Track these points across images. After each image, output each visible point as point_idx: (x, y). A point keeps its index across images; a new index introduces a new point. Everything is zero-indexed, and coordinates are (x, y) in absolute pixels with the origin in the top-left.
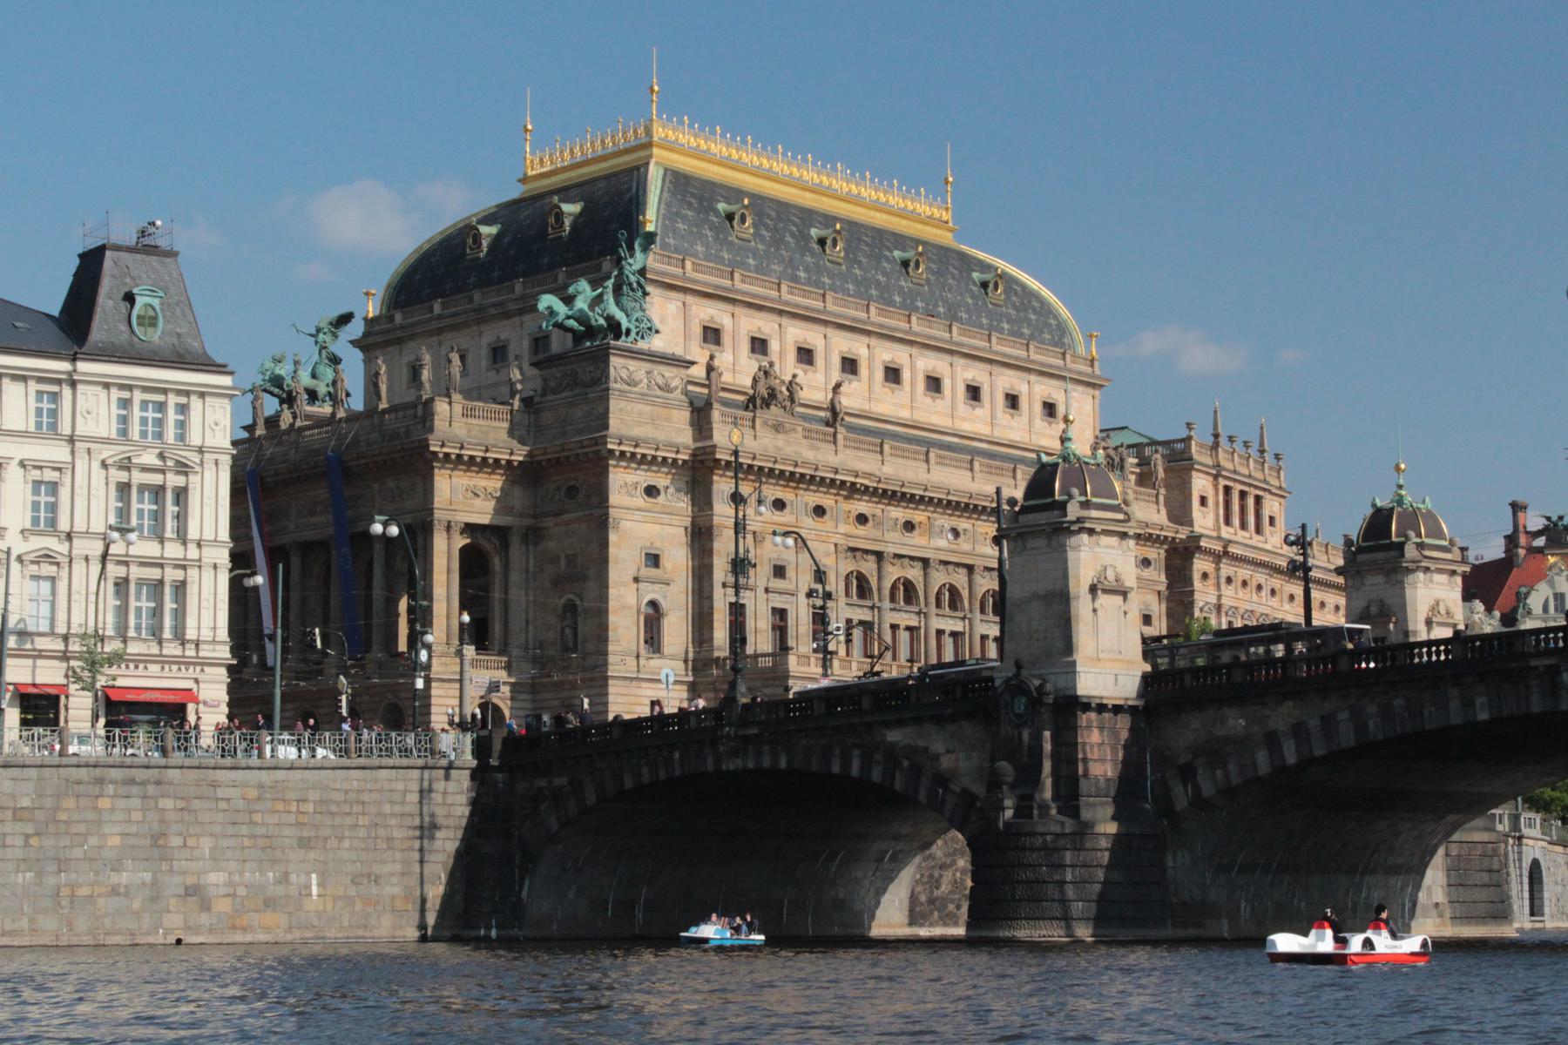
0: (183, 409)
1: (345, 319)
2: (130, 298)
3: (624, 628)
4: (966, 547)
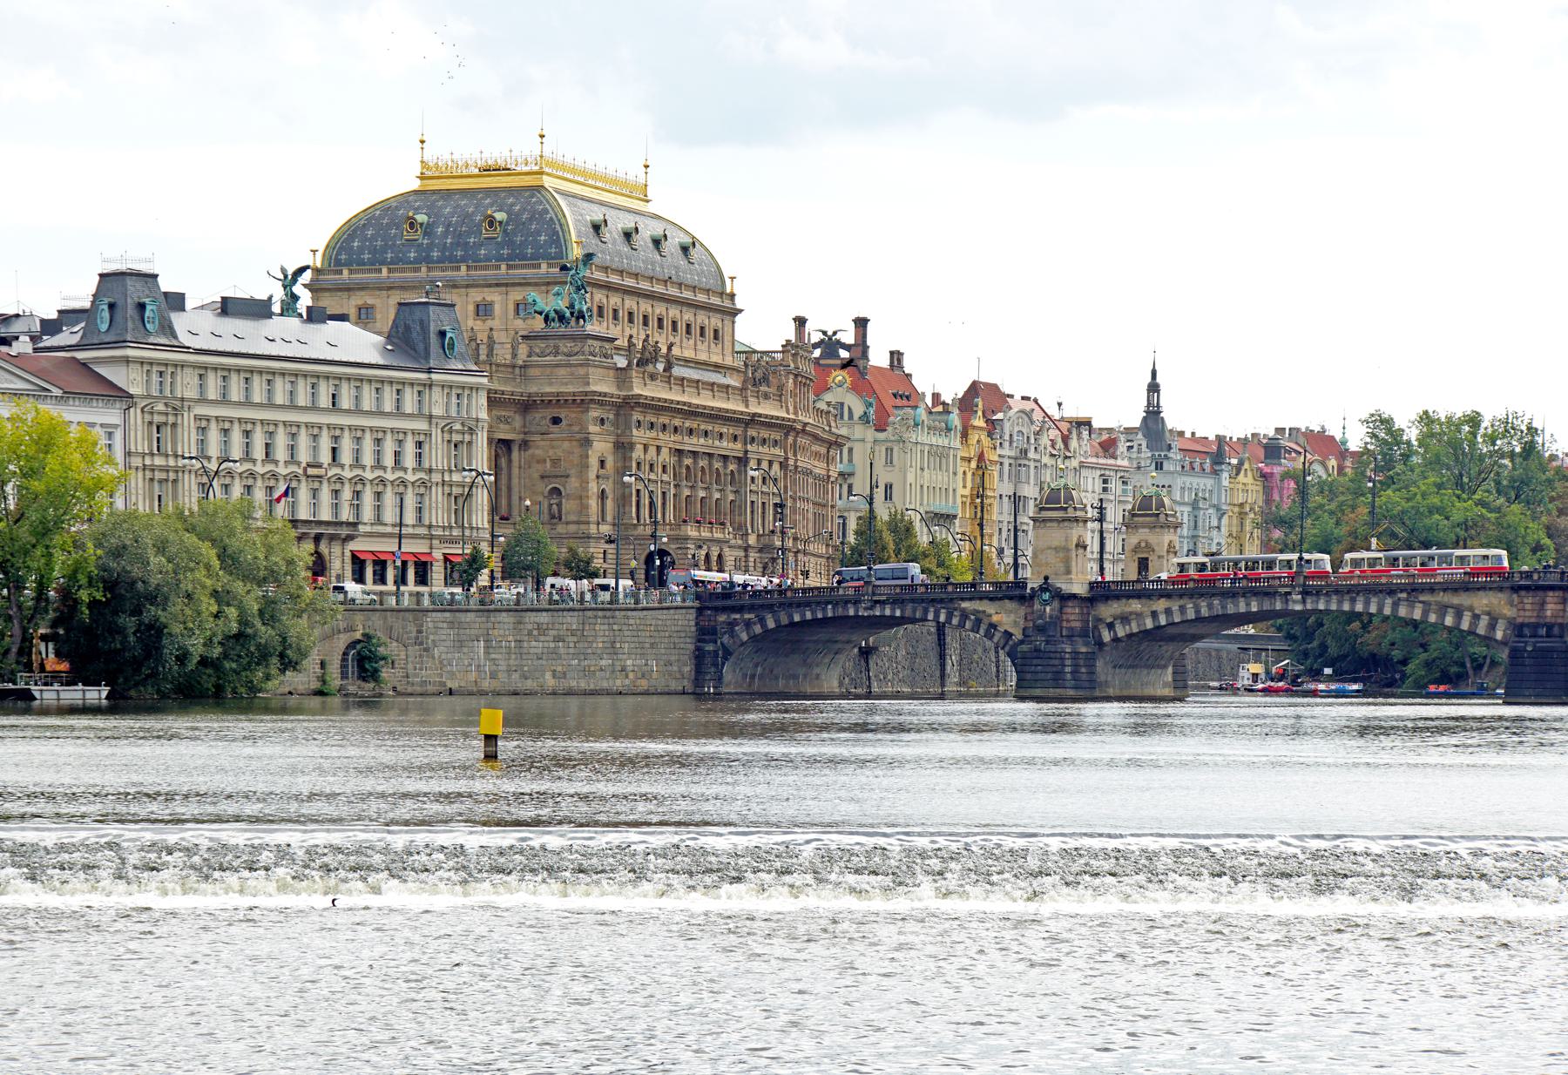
2: (442, 334)
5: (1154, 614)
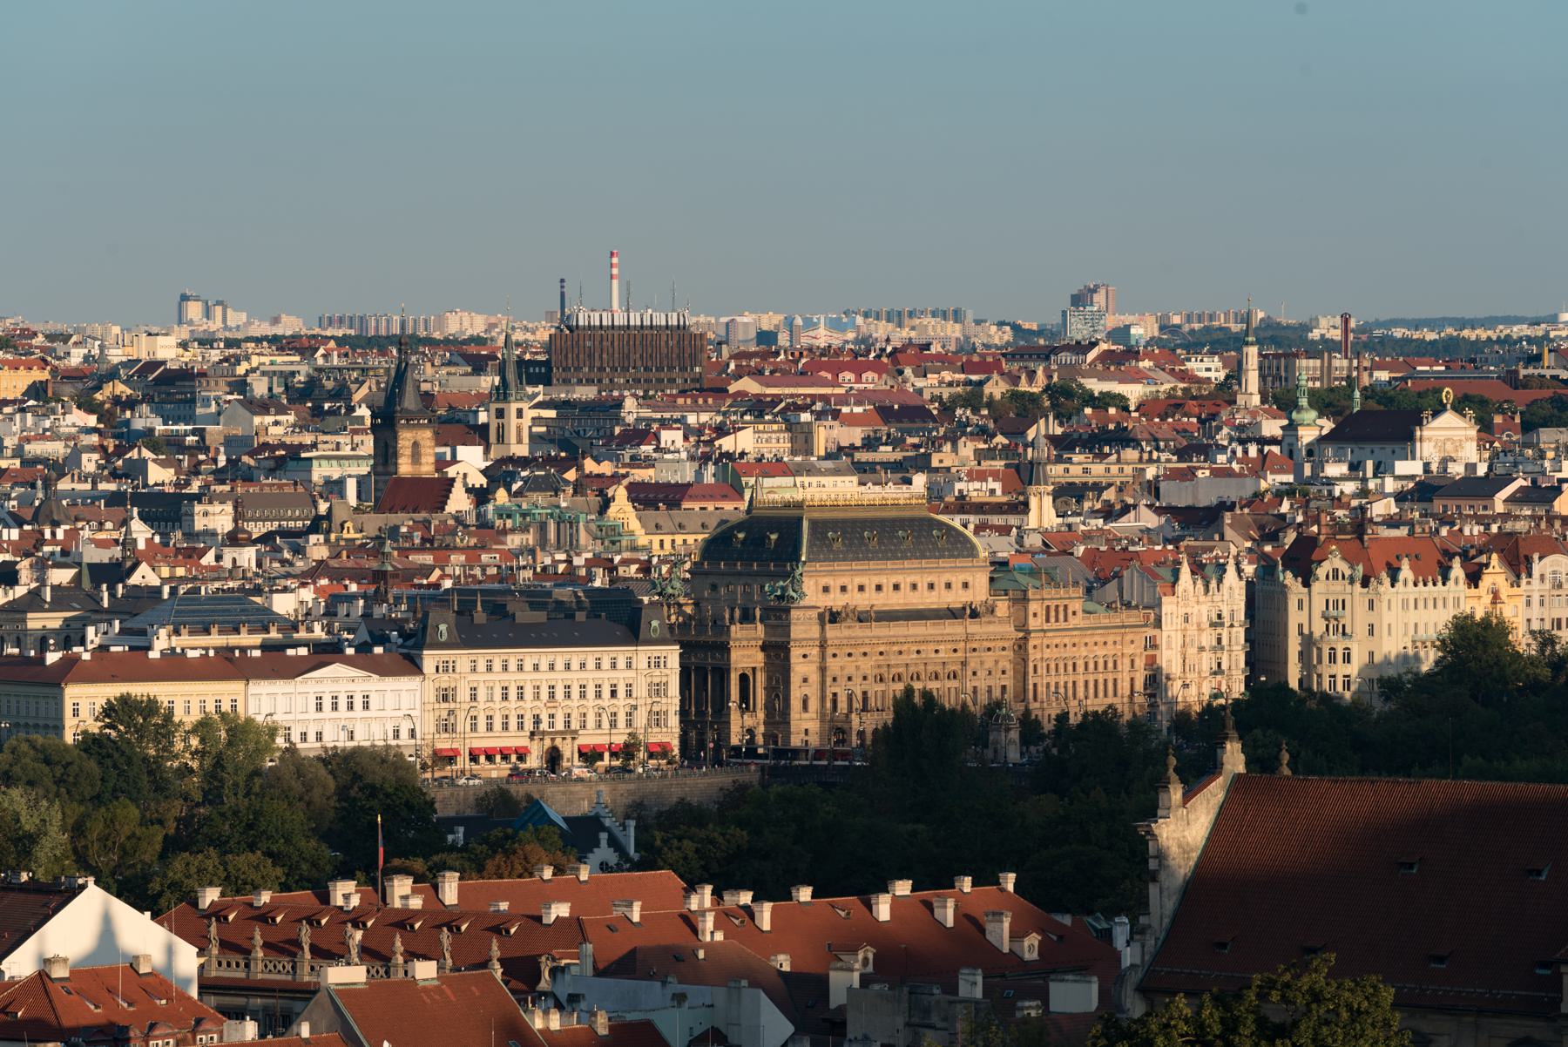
3: (796, 704)
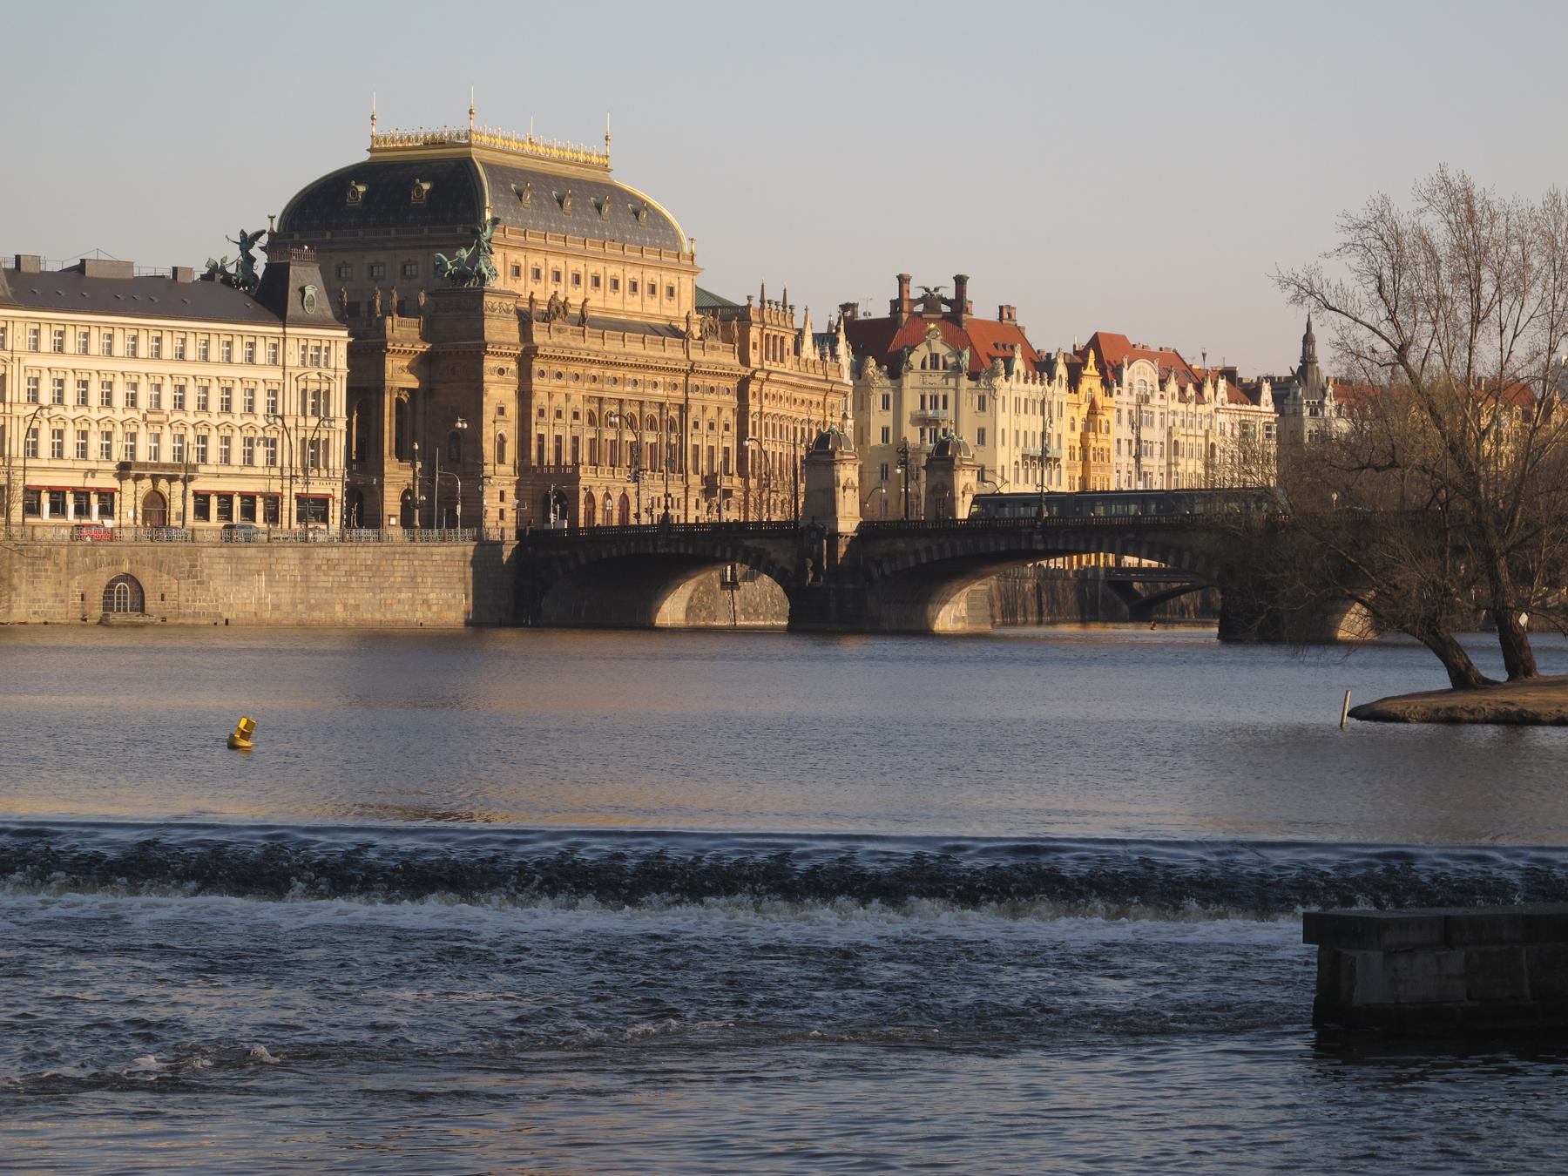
0: (328, 349)
1: (261, 233)
2: (302, 290)
3: (489, 449)
4: (640, 390)
5: (917, 553)
